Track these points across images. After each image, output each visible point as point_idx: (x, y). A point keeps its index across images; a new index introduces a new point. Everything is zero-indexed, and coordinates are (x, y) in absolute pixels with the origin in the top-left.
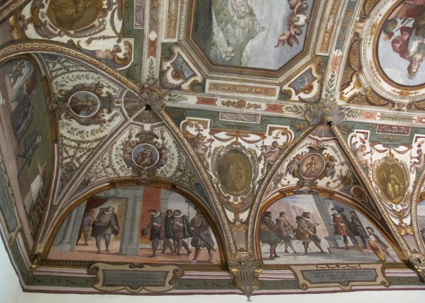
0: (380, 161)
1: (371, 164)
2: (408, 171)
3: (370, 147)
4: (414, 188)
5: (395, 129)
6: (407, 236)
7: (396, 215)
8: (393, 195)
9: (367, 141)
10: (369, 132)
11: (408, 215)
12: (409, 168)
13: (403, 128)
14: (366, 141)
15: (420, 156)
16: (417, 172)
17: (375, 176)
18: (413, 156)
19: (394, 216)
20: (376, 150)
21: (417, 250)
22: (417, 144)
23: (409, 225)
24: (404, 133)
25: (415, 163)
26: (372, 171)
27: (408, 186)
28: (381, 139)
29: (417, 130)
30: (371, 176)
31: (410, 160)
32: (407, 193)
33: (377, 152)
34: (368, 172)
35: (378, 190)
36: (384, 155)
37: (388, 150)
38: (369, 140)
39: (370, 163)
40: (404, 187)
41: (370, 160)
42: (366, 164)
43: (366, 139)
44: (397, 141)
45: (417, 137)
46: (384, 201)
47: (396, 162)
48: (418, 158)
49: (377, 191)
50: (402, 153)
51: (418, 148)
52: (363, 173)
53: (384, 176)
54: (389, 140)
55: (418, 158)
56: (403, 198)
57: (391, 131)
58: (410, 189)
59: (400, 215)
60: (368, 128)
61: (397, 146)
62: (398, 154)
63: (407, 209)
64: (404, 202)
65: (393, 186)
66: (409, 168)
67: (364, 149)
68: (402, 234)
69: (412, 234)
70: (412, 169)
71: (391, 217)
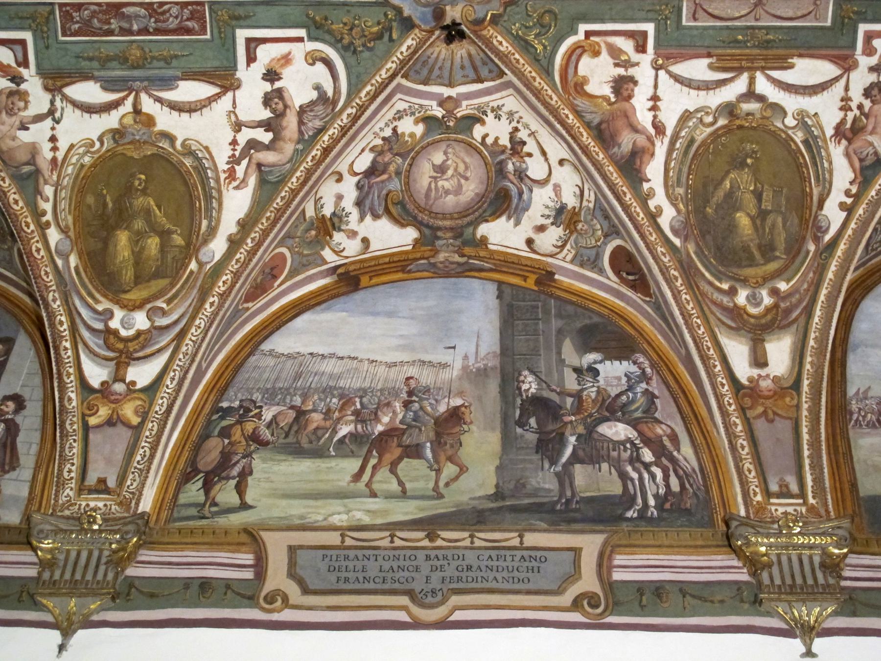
0: (92, 145)
1: (54, 160)
2: (217, 180)
3: (48, 97)
4: (234, 243)
5: (137, 16)
6: (110, 430)
7: (109, 348)
8: (128, 275)
9: (29, 74)
10: (27, 36)
11: (159, 351)
12: (222, 165)
13: (175, 10)
14: (24, 72)
15: (279, 115)
16: (262, 182)
17: (63, 205)
18: (243, 117)
19: (96, 355)
20: (76, 104)
21: (112, 483)
22: (259, 68)
23: (144, 390)
24: (188, 31)
25: (253, 145)
26: (57, 185)
27: (206, 242)
28: (91, 59)
29: (241, 11)
30: (48, 207)
31: (229, 135)
32: (193, 266)
33: (78, 112)
34: (38, 192)
35: (66, 258)
36: (112, 120)
37: (131, 99)
38: (38, 66)
39: (49, 155)
40: (188, 244)
41: (50, 145)
42: (32, 161)
43: (25, 64)
44: (162, 64)
45: (252, 44)
46: (82, 298)
47: (165, 144)
48: (267, 125)
49: (59, 262)
50: (191, 111)
51: (267, 87)
52: (12, 197)
53: (105, 205)
54: (123, 60)
55: (267, 125)
56: (172, 285)
57: (125, 25)
58: (218, 247)
59: (123, 352)
60: (17, 21)
61: (168, 83)
62: (175, 114)
63: (167, 327)
64: (169, 302)
65: (138, 238)
66: (222, 165)
67: (22, 104)
68: (93, 421)
69: (135, 420)
70: (240, 170)
71: (83, 358)
